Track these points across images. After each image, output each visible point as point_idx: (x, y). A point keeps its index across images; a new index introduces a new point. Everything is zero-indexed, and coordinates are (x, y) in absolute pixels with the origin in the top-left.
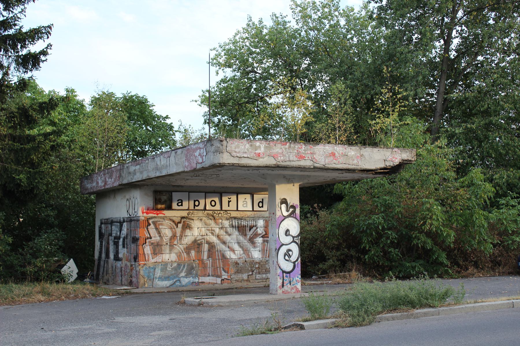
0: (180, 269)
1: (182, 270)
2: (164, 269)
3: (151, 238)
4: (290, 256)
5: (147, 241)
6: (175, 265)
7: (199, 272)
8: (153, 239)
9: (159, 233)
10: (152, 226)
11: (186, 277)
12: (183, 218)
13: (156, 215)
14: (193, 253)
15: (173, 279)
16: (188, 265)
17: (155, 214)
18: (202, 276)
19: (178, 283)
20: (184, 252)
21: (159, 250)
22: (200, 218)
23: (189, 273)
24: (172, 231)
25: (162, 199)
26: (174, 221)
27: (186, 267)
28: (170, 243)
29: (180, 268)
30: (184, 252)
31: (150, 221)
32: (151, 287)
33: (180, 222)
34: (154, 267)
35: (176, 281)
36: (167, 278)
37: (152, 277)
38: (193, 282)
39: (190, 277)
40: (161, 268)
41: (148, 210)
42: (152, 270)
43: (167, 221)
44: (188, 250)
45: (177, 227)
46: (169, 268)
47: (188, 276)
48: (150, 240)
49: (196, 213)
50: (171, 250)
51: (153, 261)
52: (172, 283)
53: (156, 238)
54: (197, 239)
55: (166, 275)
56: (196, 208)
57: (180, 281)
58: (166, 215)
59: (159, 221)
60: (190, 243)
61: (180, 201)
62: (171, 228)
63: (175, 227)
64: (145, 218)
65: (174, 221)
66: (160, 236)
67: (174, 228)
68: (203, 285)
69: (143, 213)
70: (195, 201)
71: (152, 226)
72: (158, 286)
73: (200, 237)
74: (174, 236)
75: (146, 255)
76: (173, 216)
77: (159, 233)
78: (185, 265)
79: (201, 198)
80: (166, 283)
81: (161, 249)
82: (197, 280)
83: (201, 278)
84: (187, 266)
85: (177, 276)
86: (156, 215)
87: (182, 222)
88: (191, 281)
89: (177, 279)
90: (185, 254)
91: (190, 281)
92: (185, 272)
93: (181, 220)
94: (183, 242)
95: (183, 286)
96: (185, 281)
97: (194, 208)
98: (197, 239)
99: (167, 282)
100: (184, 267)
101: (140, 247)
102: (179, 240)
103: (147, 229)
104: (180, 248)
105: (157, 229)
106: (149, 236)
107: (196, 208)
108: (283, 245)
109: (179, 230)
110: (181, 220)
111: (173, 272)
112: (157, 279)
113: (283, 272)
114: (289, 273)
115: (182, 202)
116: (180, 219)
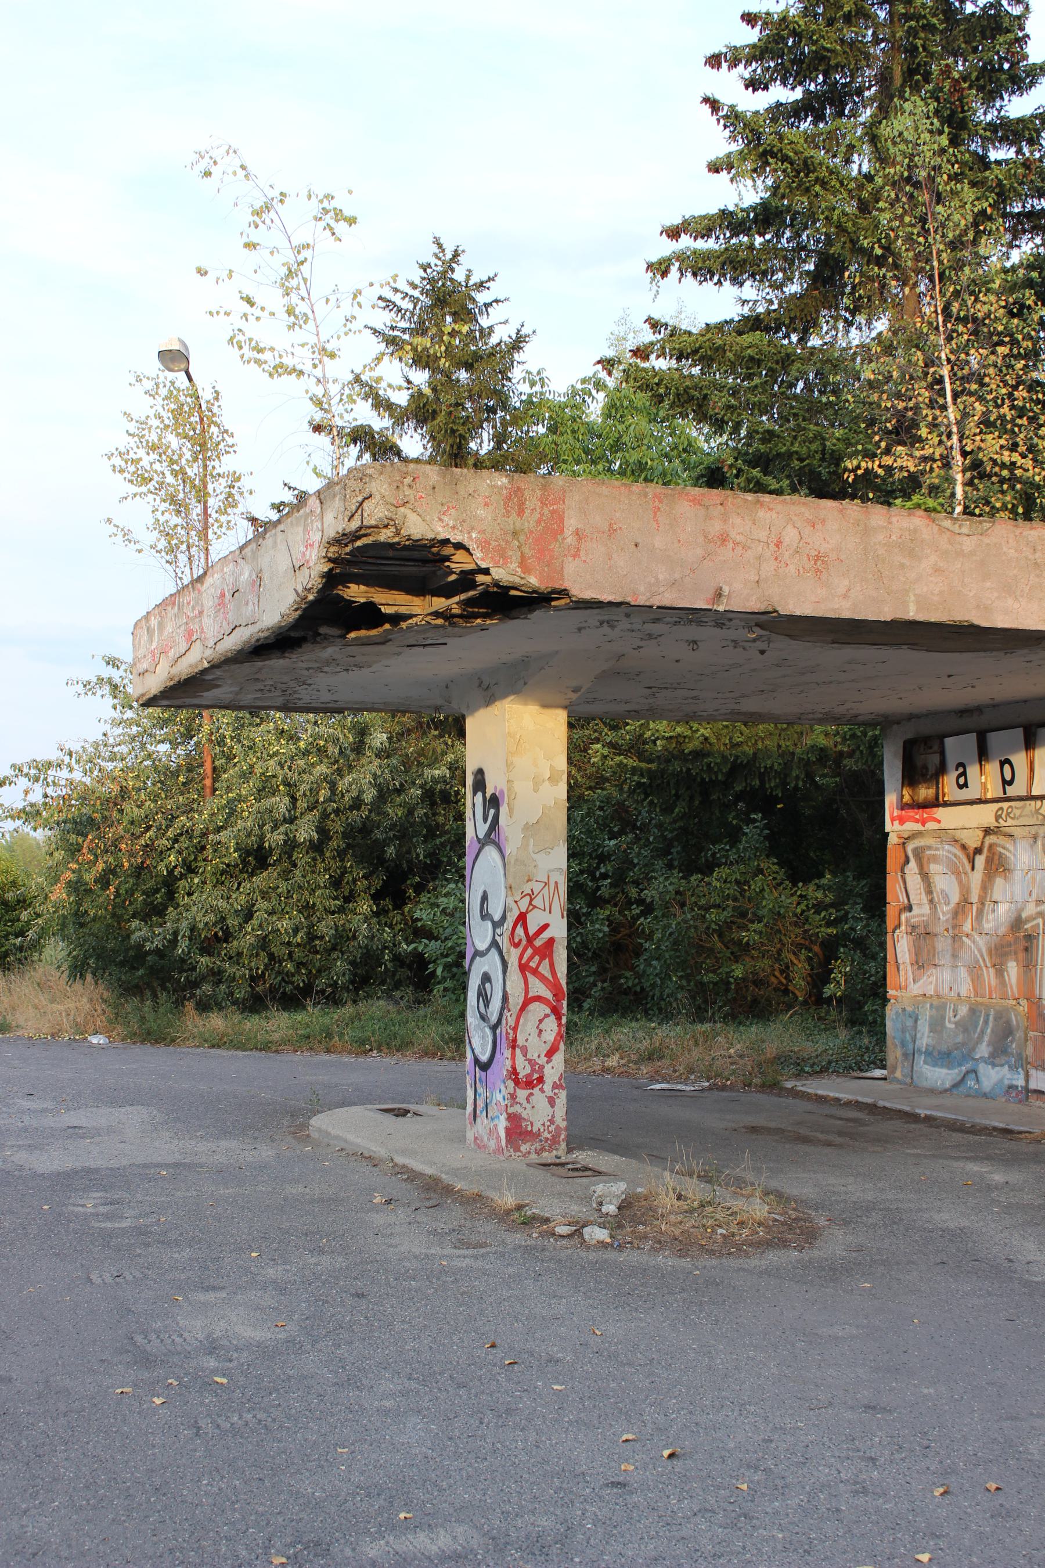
0: (976, 1027)
1: (983, 1032)
2: (937, 1025)
3: (909, 908)
4: (487, 1004)
5: (903, 917)
6: (963, 1010)
7: (1030, 1050)
8: (916, 911)
9: (929, 891)
10: (913, 864)
11: (993, 1060)
12: (987, 831)
13: (918, 827)
14: (1013, 969)
15: (960, 1065)
16: (999, 1016)
17: (917, 821)
18: (1036, 1068)
19: (971, 1083)
20: (989, 965)
21: (928, 951)
22: (1033, 830)
23: (999, 1052)
24: (960, 882)
25: (930, 767)
26: (964, 847)
27: (991, 1024)
28: (954, 927)
29: (977, 1023)
30: (989, 965)
31: (910, 848)
32: (908, 1080)
33: (978, 851)
34: (914, 1012)
35: (967, 1072)
36: (943, 1057)
37: (911, 1046)
38: (1011, 1087)
39: (1002, 1065)
40: (931, 1017)
41: (902, 809)
42: (909, 1023)
43: (947, 847)
44: (999, 953)
45: (973, 869)
46: (949, 1022)
47: (997, 1061)
48: (908, 914)
49: (1017, 812)
50: (955, 956)
51: (915, 989)
52: (959, 1078)
53: (921, 911)
54: (1024, 915)
55: (944, 1048)
56: (1011, 791)
57: (975, 1072)
58: (943, 825)
59: (929, 848)
60: (1002, 931)
61: (961, 770)
62: (957, 873)
63: (968, 867)
64: (900, 837)
65: (964, 847)
66: (931, 901)
67: (966, 873)
68: (1038, 1103)
69: (893, 820)
70: (1002, 764)
71: (913, 864)
72: (925, 1084)
73: (1030, 909)
74: (965, 902)
75: (901, 967)
76: (960, 826)
77: (929, 891)
78: (988, 1016)
79: (1015, 750)
80: (939, 1076)
81: (934, 948)
82: (1020, 1082)
83: (1033, 1072)
84: (995, 1019)
85: (968, 1056)
86: (918, 827)
87: (985, 850)
88: (1006, 1082)
89: (969, 1065)
90: (992, 971)
91: (1001, 1081)
92: (988, 1045)
93: (983, 843)
94: (988, 926)
95: (985, 1095)
96: (992, 1076)
97: (1005, 793)
98: (1024, 915)
99: (944, 1071)
100: (986, 1022)
101: (889, 937)
102: (977, 918)
103: (903, 871)
104: (977, 946)
105: (925, 876)
106: (906, 901)
107: (1011, 791)
108: (477, 954)
109: (976, 878)
110: (983, 843)
111: (960, 1038)
112: (923, 1057)
113: (477, 1061)
114: (485, 1067)
115: (964, 774)
116: (981, 834)
